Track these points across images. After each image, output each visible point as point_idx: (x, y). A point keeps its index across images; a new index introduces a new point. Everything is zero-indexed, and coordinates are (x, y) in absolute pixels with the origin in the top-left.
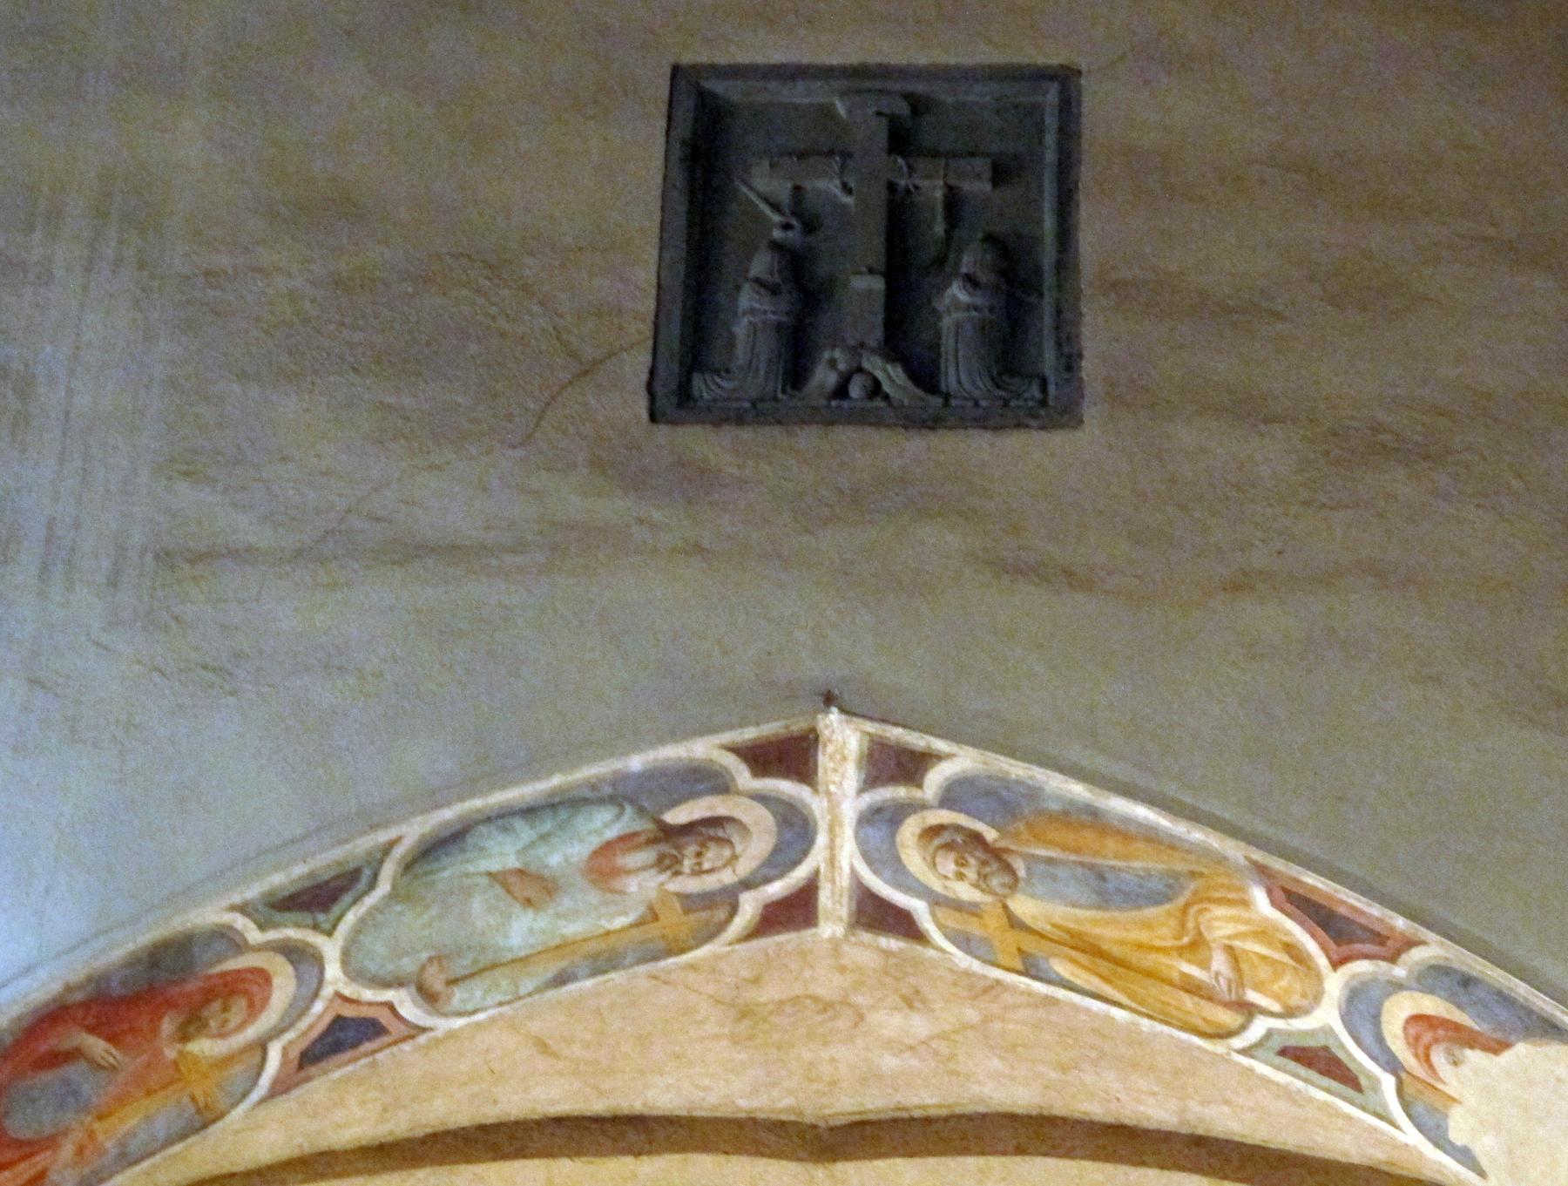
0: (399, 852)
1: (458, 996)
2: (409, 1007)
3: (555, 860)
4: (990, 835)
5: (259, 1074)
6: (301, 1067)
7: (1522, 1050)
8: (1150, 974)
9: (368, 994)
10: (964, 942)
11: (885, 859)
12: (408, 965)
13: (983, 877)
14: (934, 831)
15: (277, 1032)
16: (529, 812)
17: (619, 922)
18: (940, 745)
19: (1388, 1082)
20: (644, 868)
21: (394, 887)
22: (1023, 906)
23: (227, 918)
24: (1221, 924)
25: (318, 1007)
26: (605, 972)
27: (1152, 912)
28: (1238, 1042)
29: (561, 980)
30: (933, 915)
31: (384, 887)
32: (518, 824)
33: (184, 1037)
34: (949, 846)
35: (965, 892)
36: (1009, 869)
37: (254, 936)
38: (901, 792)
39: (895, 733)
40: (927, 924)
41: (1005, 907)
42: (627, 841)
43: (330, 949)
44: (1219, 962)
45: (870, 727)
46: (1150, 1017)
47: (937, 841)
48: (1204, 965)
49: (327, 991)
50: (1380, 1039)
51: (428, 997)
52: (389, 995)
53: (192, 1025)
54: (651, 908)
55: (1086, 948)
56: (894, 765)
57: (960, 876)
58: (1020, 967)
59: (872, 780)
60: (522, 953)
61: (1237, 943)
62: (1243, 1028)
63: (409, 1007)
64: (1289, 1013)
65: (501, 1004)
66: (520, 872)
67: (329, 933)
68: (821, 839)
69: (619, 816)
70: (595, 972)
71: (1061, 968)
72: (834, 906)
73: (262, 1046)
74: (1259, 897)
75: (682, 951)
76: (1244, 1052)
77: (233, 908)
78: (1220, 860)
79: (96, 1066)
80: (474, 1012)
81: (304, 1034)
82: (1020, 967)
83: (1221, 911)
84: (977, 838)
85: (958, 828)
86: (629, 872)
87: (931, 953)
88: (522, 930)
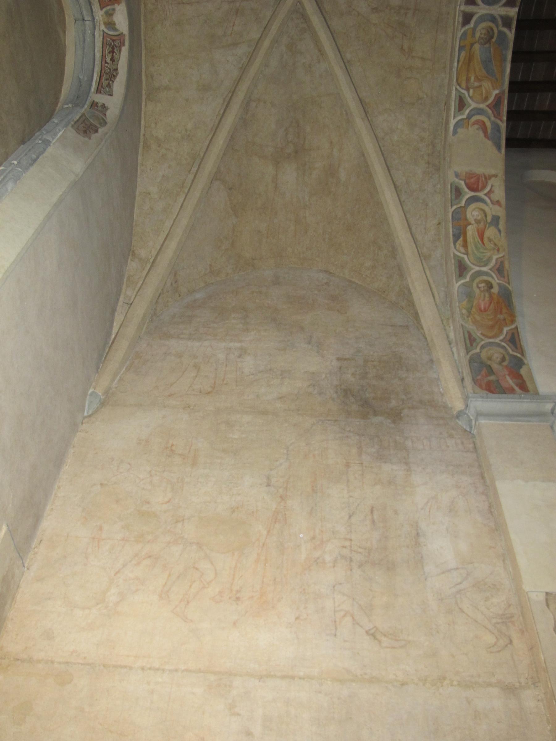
4: (494, 40)
7: (489, 143)
8: (468, 71)
10: (465, 34)
11: (482, 19)
13: (482, 38)
14: (492, 29)
18: (513, 31)
19: (464, 116)
22: (477, 47)
24: (487, 85)
27: (484, 71)
28: (458, 87)
30: (470, 28)
34: (488, 32)
35: (478, 35)
36: (486, 43)
38: (500, 22)
39: (515, 23)
40: (467, 27)
41: (475, 43)
44: (476, 84)
45: (515, 18)
46: (457, 70)
47: (489, 30)
48: (475, 81)
50: (473, 115)
55: (470, 59)
56: (506, 22)
57: (481, 34)
58: (461, 45)
59: (502, 17)
61: (483, 88)
62: (462, 88)
64: (471, 98)
68: (487, 7)
71: (463, 54)
72: (470, 9)
74: (497, 92)
76: (456, 89)
78: (503, 84)
82: (461, 45)
83: (490, 85)
84: (492, 37)
85: (494, 33)
87: (460, 28)
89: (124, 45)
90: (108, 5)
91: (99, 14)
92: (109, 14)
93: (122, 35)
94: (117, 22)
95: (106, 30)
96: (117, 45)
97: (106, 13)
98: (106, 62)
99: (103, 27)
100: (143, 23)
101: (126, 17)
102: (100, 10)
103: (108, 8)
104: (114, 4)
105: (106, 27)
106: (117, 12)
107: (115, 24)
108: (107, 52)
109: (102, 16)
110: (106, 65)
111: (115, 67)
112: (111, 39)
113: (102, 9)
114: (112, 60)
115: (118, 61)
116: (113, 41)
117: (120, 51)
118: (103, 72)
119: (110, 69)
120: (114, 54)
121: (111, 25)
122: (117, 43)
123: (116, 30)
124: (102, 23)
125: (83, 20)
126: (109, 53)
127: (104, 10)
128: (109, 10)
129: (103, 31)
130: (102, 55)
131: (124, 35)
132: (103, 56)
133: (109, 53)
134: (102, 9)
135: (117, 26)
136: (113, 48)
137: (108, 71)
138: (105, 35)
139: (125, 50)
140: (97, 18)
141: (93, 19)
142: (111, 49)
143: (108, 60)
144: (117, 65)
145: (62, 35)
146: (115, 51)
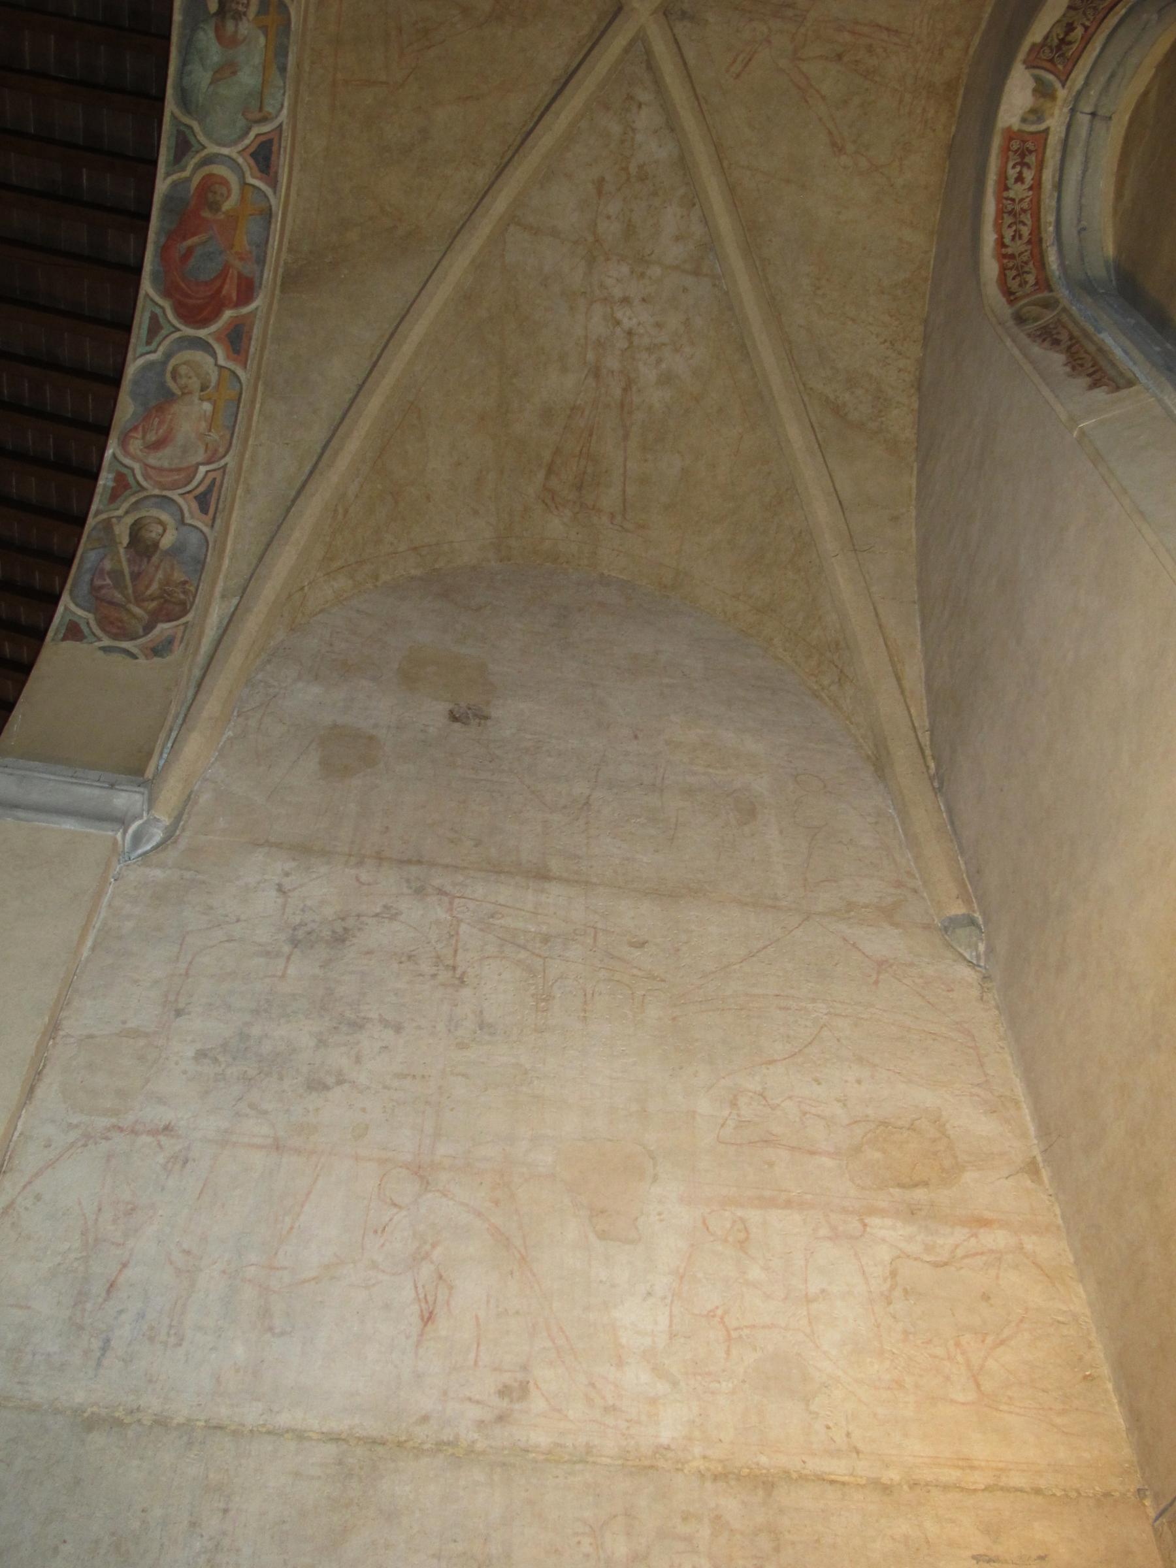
0: (178, 113)
1: (268, 109)
2: (266, 128)
3: (216, 59)
5: (259, 189)
6: (268, 174)
9: (247, 142)
12: (241, 123)
15: (242, 176)
16: (184, 63)
17: (262, 40)
20: (237, 26)
21: (196, 119)
23: (169, 180)
25: (240, 160)
26: (287, 53)
29: (283, 69)
31: (195, 125)
32: (189, 68)
33: (218, 209)
37: (186, 174)
42: (217, 30)
43: (212, 149)
49: (234, 155)
51: (264, 120)
52: (252, 135)
53: (215, 207)
54: (260, 28)
60: (260, 80)
63: (266, 128)
65: (284, 94)
66: (216, 72)
67: (204, 147)
69: (204, 30)
70: (286, 55)
73: (244, 184)
75: (289, 20)
77: (165, 179)
79: (204, 243)
80: (282, 105)
81: (251, 169)
86: (236, 32)
88: (248, 78)
89: (1034, 46)
90: (1032, 133)
91: (1055, 122)
92: (1036, 114)
93: (1030, 65)
94: (1029, 92)
95: (1058, 85)
96: (1047, 51)
97: (1040, 120)
98: (1086, 28)
99: (1062, 93)
100: (986, 16)
101: (1005, 99)
102: (1052, 129)
103: (1033, 128)
104: (1020, 131)
105: (1055, 90)
106: (1021, 112)
107: (1035, 91)
108: (1075, 46)
109: (1052, 115)
110: (1087, 23)
111: (1073, 13)
112: (1055, 65)
113: (1047, 130)
114: (1070, 28)
115: (1058, 21)
116: (1051, 61)
117: (1046, 38)
118: (1102, 15)
119: (1084, 13)
120: (1061, 36)
121: (1043, 91)
122: (1047, 54)
123: (1038, 80)
124: (1059, 102)
125: (1093, 115)
126: (1070, 43)
127: (1042, 127)
128: (1033, 123)
129: (1063, 86)
130: (1087, 43)
131: (1025, 62)
132: (1087, 41)
133: (1070, 43)
134: (1047, 130)
135: (1031, 84)
136: (1059, 48)
137: (1090, 12)
138: (1063, 78)
139: (1037, 33)
140: (1066, 110)
141: (1073, 111)
142: (1064, 48)
143: (1079, 32)
144: (1064, 15)
145: (1153, 96)
146: (1056, 42)
